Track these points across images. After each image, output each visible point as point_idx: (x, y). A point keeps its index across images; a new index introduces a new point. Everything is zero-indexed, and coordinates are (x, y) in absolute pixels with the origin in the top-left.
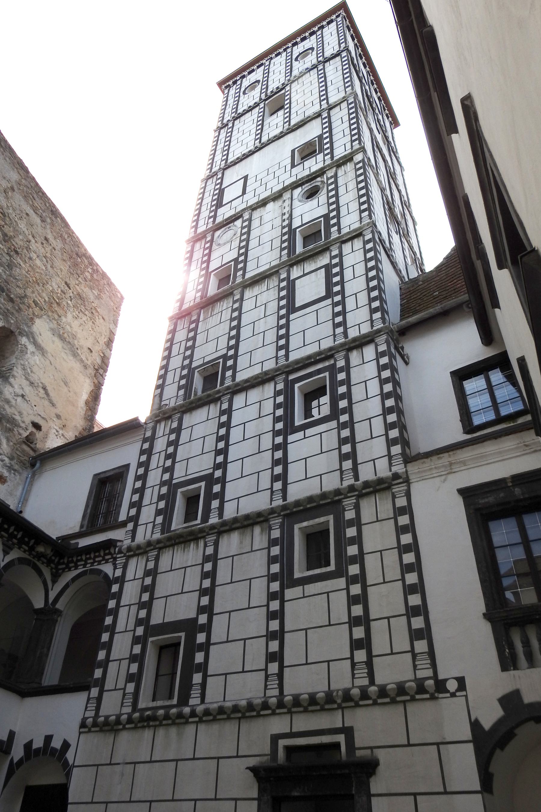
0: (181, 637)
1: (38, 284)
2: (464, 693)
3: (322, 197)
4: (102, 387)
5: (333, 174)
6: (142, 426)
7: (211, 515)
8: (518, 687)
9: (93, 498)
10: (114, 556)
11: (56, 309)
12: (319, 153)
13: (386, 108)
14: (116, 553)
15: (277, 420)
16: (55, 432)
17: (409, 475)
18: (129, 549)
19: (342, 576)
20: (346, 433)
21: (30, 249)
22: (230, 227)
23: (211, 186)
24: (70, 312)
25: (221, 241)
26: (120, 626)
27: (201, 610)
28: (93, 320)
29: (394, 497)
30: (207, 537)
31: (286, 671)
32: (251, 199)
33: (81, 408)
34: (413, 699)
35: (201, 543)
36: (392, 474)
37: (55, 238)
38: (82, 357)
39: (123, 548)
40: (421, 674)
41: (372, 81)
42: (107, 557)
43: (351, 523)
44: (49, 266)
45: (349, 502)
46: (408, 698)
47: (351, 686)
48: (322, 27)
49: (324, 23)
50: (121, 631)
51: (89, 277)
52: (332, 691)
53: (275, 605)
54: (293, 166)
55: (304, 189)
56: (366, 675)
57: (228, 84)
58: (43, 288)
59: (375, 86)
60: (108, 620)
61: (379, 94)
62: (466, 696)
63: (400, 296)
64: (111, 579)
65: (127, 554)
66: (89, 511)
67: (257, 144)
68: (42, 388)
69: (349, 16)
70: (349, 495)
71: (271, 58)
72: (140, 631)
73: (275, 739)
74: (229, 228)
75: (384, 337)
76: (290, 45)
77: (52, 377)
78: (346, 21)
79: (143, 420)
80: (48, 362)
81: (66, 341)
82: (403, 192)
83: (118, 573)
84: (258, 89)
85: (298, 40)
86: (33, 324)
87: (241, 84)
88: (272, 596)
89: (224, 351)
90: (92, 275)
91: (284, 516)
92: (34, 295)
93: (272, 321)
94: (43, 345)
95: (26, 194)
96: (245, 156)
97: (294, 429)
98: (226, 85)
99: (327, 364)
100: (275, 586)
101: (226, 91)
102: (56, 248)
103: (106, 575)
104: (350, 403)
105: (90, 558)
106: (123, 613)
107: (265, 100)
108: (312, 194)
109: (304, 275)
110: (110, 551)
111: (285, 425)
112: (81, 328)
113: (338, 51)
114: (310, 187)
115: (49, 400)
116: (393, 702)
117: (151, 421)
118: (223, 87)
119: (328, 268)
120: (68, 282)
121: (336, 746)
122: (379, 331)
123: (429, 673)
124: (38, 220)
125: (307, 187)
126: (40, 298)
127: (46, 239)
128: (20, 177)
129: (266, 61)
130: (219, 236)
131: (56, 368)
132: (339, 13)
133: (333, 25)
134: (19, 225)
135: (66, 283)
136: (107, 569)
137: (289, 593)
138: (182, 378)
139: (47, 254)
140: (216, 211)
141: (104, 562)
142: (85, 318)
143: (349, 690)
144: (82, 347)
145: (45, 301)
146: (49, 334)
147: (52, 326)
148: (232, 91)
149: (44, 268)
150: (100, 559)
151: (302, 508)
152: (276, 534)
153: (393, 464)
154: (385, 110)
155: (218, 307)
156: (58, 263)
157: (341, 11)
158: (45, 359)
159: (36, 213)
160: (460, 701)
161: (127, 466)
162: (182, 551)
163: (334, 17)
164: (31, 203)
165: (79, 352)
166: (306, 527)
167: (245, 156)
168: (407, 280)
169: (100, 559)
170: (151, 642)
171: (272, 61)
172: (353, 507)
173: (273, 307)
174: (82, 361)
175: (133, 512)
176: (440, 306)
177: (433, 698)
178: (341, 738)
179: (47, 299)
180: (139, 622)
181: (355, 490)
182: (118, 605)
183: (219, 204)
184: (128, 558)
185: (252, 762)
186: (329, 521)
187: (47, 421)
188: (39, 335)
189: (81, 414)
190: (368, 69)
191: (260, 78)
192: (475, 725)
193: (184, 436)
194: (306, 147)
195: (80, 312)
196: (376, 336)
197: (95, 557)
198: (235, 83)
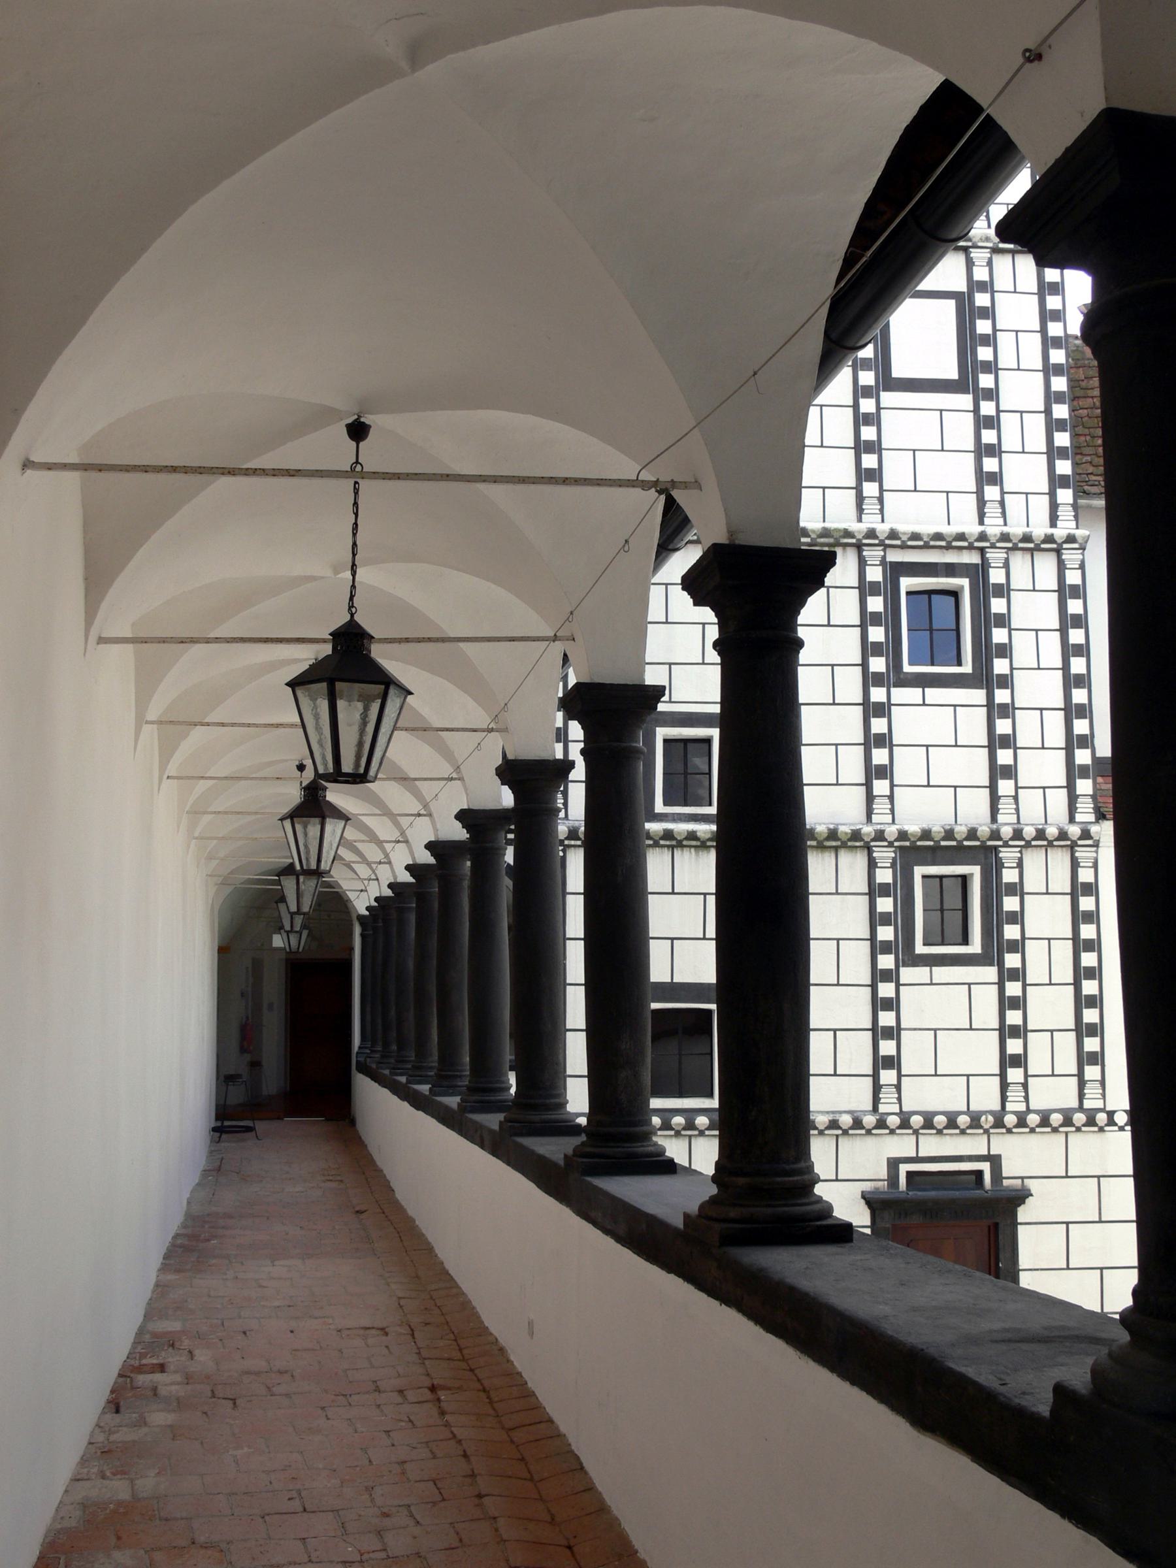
65: (566, 842)
73: (894, 1164)
91: (900, 848)
116: (1055, 1130)
121: (979, 1174)
162: (693, 860)
177: (1101, 1130)
178: (985, 1167)
185: (867, 1186)
196: (1065, 546)
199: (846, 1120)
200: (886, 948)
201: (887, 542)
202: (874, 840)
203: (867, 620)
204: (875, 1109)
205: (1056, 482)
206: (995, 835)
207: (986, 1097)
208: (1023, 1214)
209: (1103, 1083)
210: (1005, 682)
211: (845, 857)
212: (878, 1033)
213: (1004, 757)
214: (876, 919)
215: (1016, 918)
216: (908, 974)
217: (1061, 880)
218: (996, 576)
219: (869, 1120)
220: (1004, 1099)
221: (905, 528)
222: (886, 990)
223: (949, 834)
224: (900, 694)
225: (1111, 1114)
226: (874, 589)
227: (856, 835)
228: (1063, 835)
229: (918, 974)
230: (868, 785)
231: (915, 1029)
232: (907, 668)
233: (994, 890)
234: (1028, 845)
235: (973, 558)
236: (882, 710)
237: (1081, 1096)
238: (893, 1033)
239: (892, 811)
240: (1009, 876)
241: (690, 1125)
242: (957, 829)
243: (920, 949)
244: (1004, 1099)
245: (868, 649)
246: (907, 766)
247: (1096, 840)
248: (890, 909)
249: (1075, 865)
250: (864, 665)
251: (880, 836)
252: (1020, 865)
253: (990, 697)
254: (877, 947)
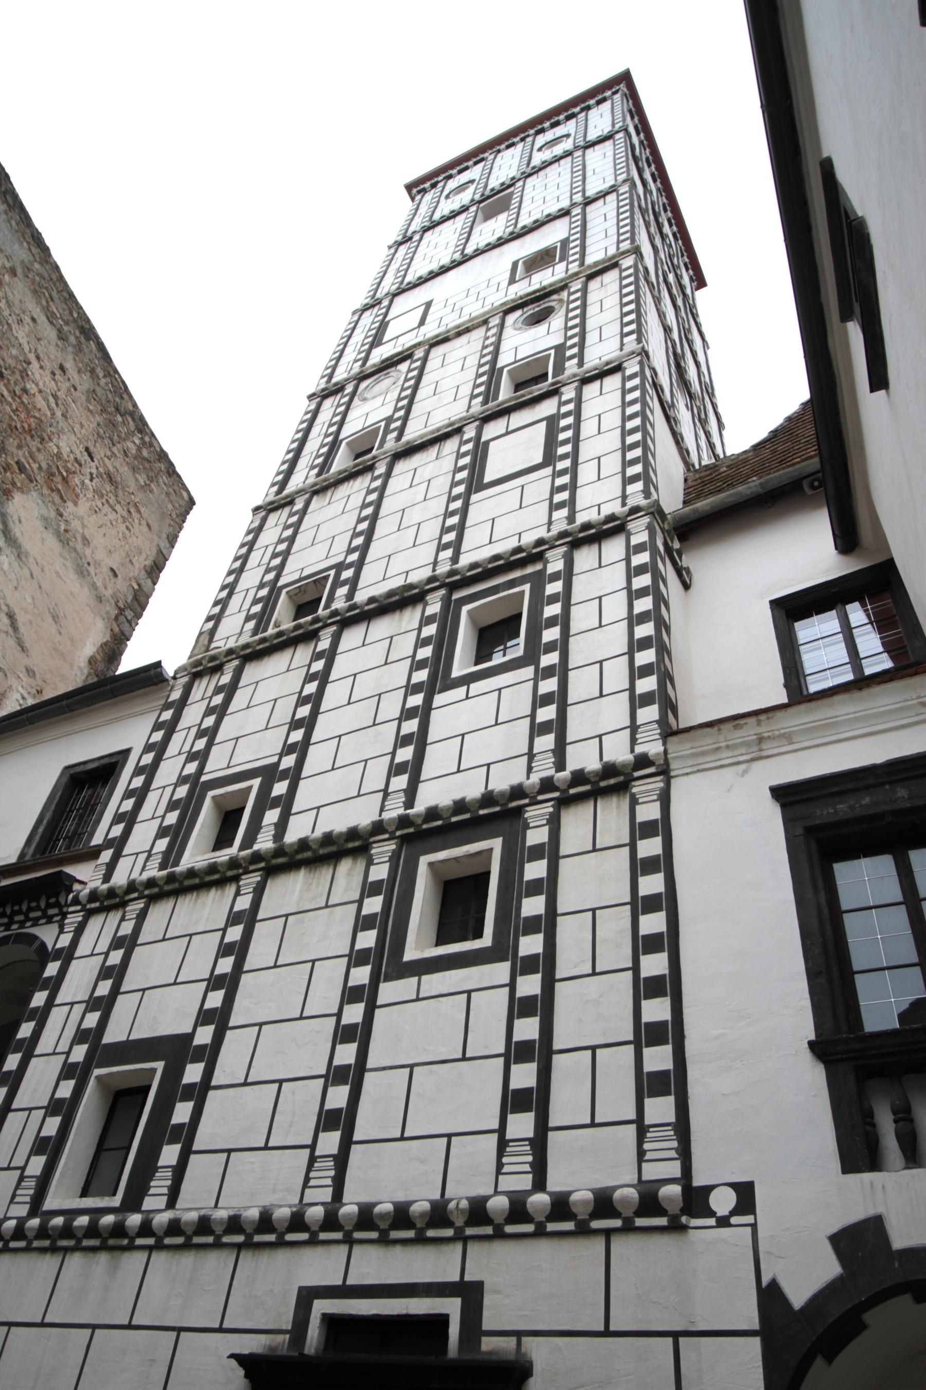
0: (154, 1070)
1: (32, 437)
2: (749, 1219)
3: (557, 321)
4: (128, 642)
5: (579, 286)
6: (167, 680)
7: (259, 836)
8: (880, 1210)
9: (53, 807)
10: (65, 910)
11: (60, 487)
12: (561, 261)
13: (685, 254)
14: (69, 902)
15: (417, 665)
16: (19, 698)
17: (671, 761)
18: (94, 896)
19: (503, 959)
20: (549, 685)
21: (27, 375)
22: (388, 373)
23: (368, 319)
24: (85, 499)
25: (367, 395)
26: (45, 1044)
27: (205, 1017)
28: (128, 524)
29: (634, 802)
30: (243, 877)
31: (356, 1152)
32: (431, 330)
33: (80, 668)
34: (628, 1228)
35: (231, 890)
36: (635, 757)
37: (79, 372)
38: (95, 579)
39: (82, 894)
40: (651, 1172)
41: (664, 205)
42: (51, 912)
43: (536, 853)
44: (59, 414)
45: (537, 814)
46: (617, 1223)
47: (491, 1191)
48: (588, 108)
49: (592, 102)
50: (45, 1052)
51: (134, 452)
52: (450, 1200)
53: (354, 1014)
54: (512, 281)
55: (526, 312)
56: (527, 1168)
57: (422, 187)
58: (39, 445)
59: (670, 214)
60: (26, 1030)
61: (675, 228)
62: (754, 1226)
63: (684, 490)
64: (50, 949)
65: (88, 906)
66: (41, 830)
67: (457, 256)
68: (7, 614)
69: (633, 95)
70: (540, 798)
71: (499, 151)
72: (79, 1054)
73: (307, 1296)
74: (386, 374)
75: (647, 520)
76: (532, 132)
77: (29, 600)
78: (628, 101)
79: (169, 669)
80: (26, 572)
81: (68, 544)
82: (704, 368)
83: (65, 941)
84: (472, 188)
85: (547, 125)
86: (8, 499)
87: (444, 187)
88: (351, 995)
89: (340, 558)
90: (139, 449)
92: (20, 453)
93: (438, 506)
94: (21, 540)
95: (37, 288)
96: (433, 275)
97: (448, 682)
98: (419, 188)
99: (530, 570)
100: (361, 975)
101: (418, 197)
102: (79, 387)
103: (43, 945)
104: (566, 634)
105: (19, 912)
106: (56, 1016)
107: (480, 202)
108: (537, 319)
109: (508, 433)
110: (57, 901)
111: (433, 677)
112: (102, 531)
113: (609, 132)
114: (537, 309)
115: (17, 638)
116: (583, 1231)
117: (185, 673)
118: (414, 191)
119: (552, 422)
120: (92, 449)
122: (635, 510)
123: (674, 1169)
124: (52, 334)
125: (530, 310)
126: (31, 461)
127: (62, 368)
128: (31, 258)
129: (491, 154)
130: (368, 386)
131: (40, 587)
132: (618, 88)
133: (607, 105)
134: (14, 332)
135: (87, 449)
136: (47, 934)
137: (388, 991)
138: (255, 602)
139: (59, 394)
140: (369, 352)
141: (43, 921)
142: (112, 516)
143: (486, 1199)
144: (98, 564)
145: (40, 468)
146: (39, 524)
147: (44, 512)
148: (428, 197)
149: (49, 414)
150: (39, 914)
151: (439, 823)
152: (380, 872)
153: (639, 741)
154: (683, 256)
155: (344, 490)
156: (76, 411)
157: (622, 85)
158: (22, 565)
159: (51, 323)
160: (737, 1236)
161: (126, 752)
163: (608, 93)
164: (44, 303)
165: (92, 569)
166: (443, 861)
167: (433, 275)
168: (697, 467)
169: (39, 914)
170: (97, 1077)
171: (500, 155)
172: (545, 822)
173: (441, 485)
174: (94, 586)
175: (117, 830)
176: (759, 481)
177: (676, 1227)
178: (452, 1307)
179: (44, 466)
180: (81, 1036)
181: (556, 789)
182: (50, 1003)
183: (377, 340)
184: (89, 914)
186: (491, 849)
187: (6, 675)
188: (17, 522)
189: (78, 679)
190: (659, 185)
191: (477, 178)
193: (240, 698)
194: (539, 258)
195: (105, 503)
196: (629, 518)
197: (30, 909)
198: (434, 186)
231: (384, 1069)
247: (659, 765)
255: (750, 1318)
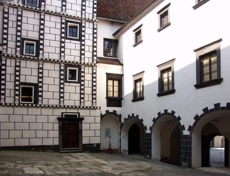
34: (92, 109)
73: (62, 113)
116: (88, 109)
177: (95, 109)
178: (77, 114)
185: (58, 117)
192: (101, 114)
199: (55, 106)
200: (62, 79)
201: (66, 16)
202: (61, 62)
203: (62, 28)
204: (60, 104)
205: (94, 12)
206: (81, 63)
207: (77, 104)
208: (83, 122)
209: (96, 102)
210: (84, 41)
211: (56, 65)
212: (60, 93)
213: (83, 52)
214: (61, 75)
215: (83, 76)
216: (65, 84)
217: (91, 72)
218: (83, 25)
219: (59, 106)
220: (80, 104)
221: (69, 15)
222: (62, 86)
223: (73, 62)
224: (66, 41)
225: (97, 107)
226: (63, 23)
227: (58, 61)
228: (91, 65)
229: (68, 84)
230: (60, 54)
232: (68, 37)
233: (80, 72)
234: (86, 66)
235: (79, 21)
236: (64, 42)
237: (93, 104)
238: (63, 93)
239: (64, 58)
240: (83, 70)
241: (28, 106)
242: (75, 62)
243: (68, 80)
244: (80, 104)
245: (62, 33)
246: (67, 52)
248: (63, 73)
249: (93, 70)
250: (61, 35)
251: (62, 61)
252: (84, 69)
253: (81, 43)
254: (61, 79)
255: (100, 116)
